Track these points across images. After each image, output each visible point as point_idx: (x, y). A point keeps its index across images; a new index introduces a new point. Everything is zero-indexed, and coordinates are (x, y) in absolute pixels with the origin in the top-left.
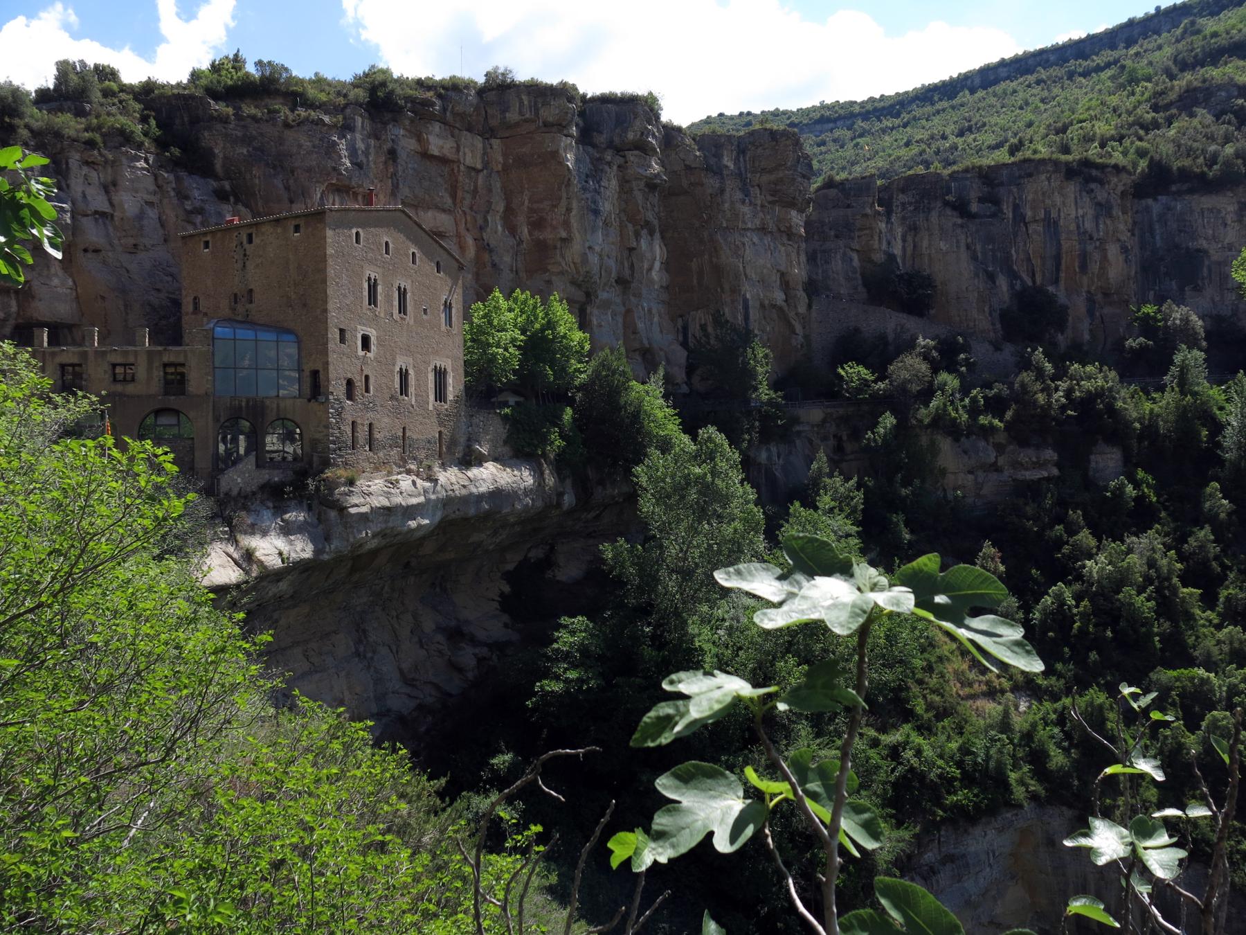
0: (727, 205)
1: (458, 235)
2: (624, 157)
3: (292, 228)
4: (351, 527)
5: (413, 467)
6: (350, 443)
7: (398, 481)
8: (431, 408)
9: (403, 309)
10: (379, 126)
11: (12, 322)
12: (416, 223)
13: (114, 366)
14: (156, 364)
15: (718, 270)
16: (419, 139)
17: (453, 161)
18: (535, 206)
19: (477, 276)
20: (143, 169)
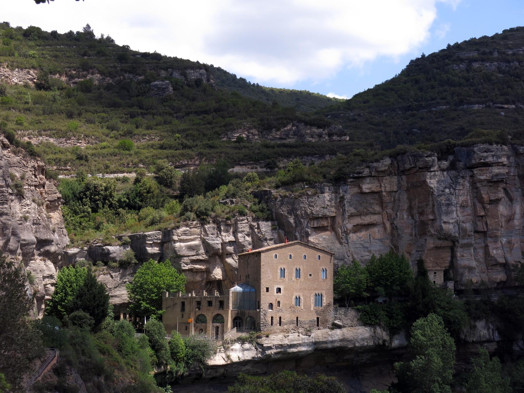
1: (384, 223)
6: (270, 323)
7: (288, 336)
8: (312, 309)
9: (298, 275)
11: (204, 282)
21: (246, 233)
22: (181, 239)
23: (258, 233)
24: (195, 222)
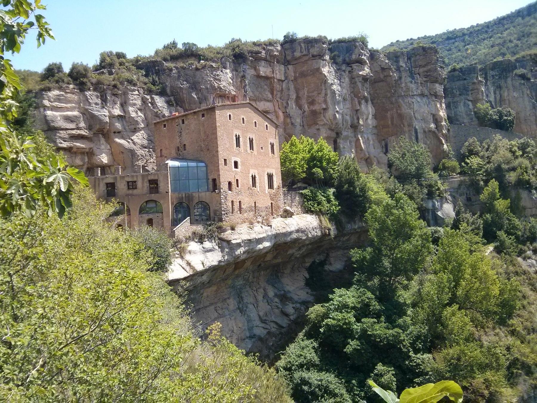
0: (403, 85)
1: (275, 111)
2: (351, 67)
3: (201, 115)
4: (234, 249)
5: (260, 220)
6: (231, 211)
8: (267, 192)
9: (252, 147)
10: (237, 65)
12: (255, 108)
13: (128, 182)
14: (146, 180)
15: (401, 116)
16: (255, 69)
17: (271, 78)
18: (310, 94)
19: (285, 129)
20: (137, 95)
21: (138, 106)
22: (53, 106)
23: (154, 108)
24: (71, 86)
